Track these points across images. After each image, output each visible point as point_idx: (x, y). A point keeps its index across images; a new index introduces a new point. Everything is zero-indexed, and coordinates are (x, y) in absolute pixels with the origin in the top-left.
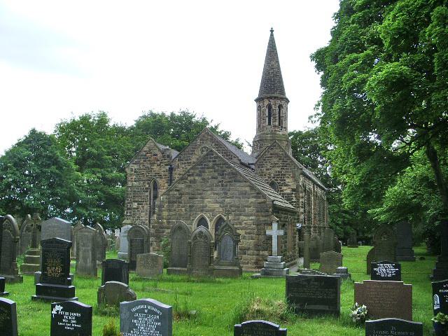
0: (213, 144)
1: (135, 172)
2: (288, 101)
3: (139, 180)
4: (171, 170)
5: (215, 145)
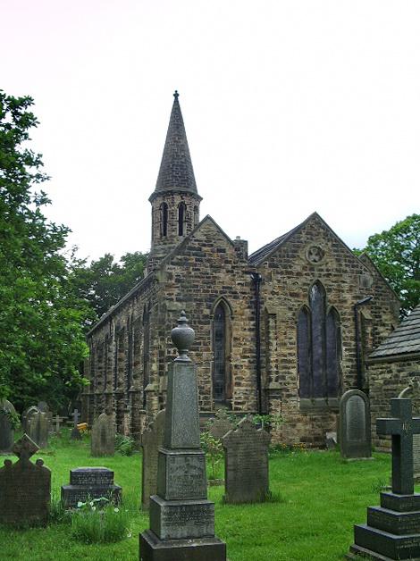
0: (330, 244)
1: (178, 281)
2: (200, 199)
3: (187, 299)
4: (257, 282)
5: (333, 246)
